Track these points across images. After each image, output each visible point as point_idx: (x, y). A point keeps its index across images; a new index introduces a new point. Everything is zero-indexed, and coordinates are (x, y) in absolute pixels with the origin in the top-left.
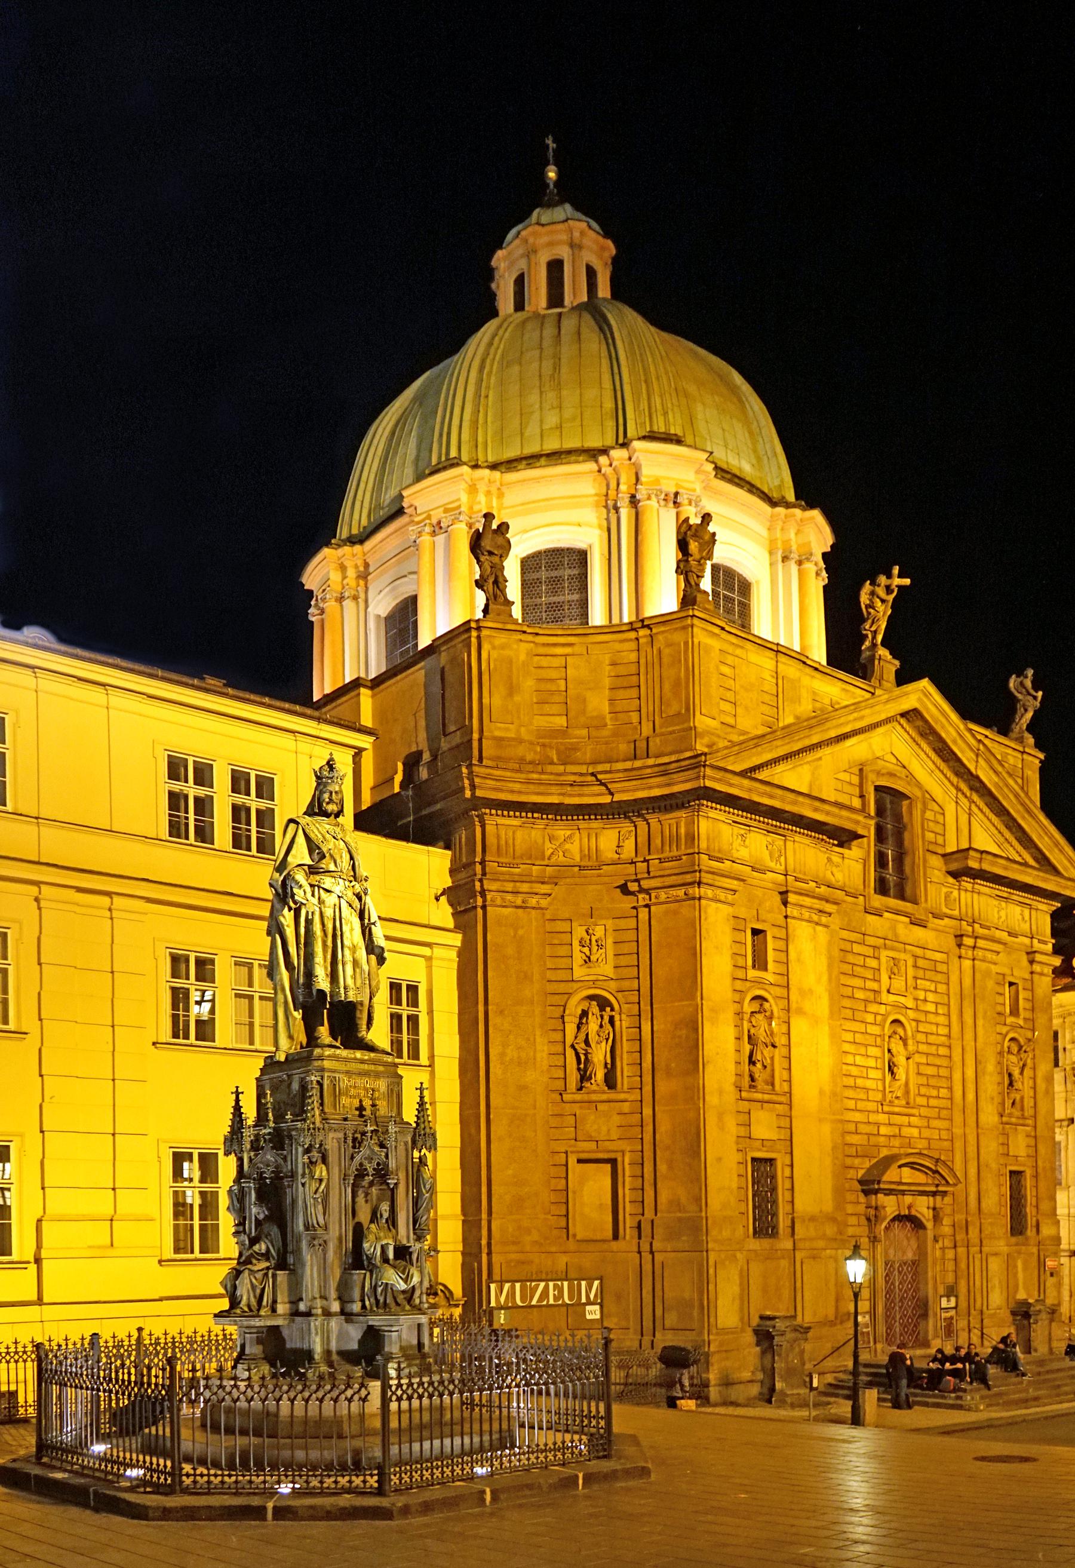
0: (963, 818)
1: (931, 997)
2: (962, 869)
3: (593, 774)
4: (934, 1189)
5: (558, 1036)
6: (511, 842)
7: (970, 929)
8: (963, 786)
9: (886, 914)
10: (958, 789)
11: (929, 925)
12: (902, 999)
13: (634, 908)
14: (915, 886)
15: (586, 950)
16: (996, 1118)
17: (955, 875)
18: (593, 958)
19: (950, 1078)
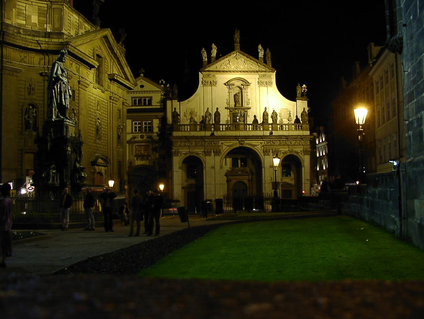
0: (112, 64)
1: (105, 112)
2: (112, 79)
3: (37, 41)
4: (105, 165)
5: (20, 115)
6: (10, 56)
7: (112, 94)
8: (113, 56)
9: (97, 89)
10: (111, 57)
11: (105, 93)
12: (99, 112)
13: (44, 80)
14: (102, 81)
15: (29, 90)
16: (116, 147)
17: (110, 80)
18: (31, 93)
19: (108, 135)
